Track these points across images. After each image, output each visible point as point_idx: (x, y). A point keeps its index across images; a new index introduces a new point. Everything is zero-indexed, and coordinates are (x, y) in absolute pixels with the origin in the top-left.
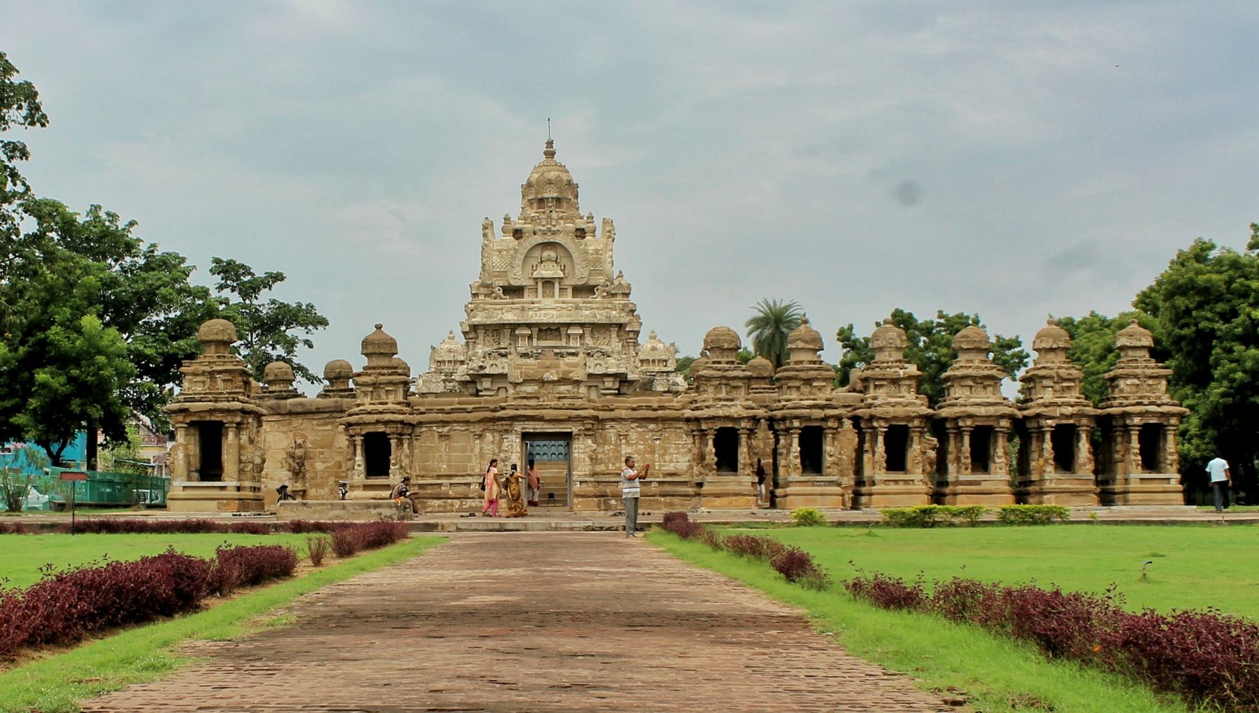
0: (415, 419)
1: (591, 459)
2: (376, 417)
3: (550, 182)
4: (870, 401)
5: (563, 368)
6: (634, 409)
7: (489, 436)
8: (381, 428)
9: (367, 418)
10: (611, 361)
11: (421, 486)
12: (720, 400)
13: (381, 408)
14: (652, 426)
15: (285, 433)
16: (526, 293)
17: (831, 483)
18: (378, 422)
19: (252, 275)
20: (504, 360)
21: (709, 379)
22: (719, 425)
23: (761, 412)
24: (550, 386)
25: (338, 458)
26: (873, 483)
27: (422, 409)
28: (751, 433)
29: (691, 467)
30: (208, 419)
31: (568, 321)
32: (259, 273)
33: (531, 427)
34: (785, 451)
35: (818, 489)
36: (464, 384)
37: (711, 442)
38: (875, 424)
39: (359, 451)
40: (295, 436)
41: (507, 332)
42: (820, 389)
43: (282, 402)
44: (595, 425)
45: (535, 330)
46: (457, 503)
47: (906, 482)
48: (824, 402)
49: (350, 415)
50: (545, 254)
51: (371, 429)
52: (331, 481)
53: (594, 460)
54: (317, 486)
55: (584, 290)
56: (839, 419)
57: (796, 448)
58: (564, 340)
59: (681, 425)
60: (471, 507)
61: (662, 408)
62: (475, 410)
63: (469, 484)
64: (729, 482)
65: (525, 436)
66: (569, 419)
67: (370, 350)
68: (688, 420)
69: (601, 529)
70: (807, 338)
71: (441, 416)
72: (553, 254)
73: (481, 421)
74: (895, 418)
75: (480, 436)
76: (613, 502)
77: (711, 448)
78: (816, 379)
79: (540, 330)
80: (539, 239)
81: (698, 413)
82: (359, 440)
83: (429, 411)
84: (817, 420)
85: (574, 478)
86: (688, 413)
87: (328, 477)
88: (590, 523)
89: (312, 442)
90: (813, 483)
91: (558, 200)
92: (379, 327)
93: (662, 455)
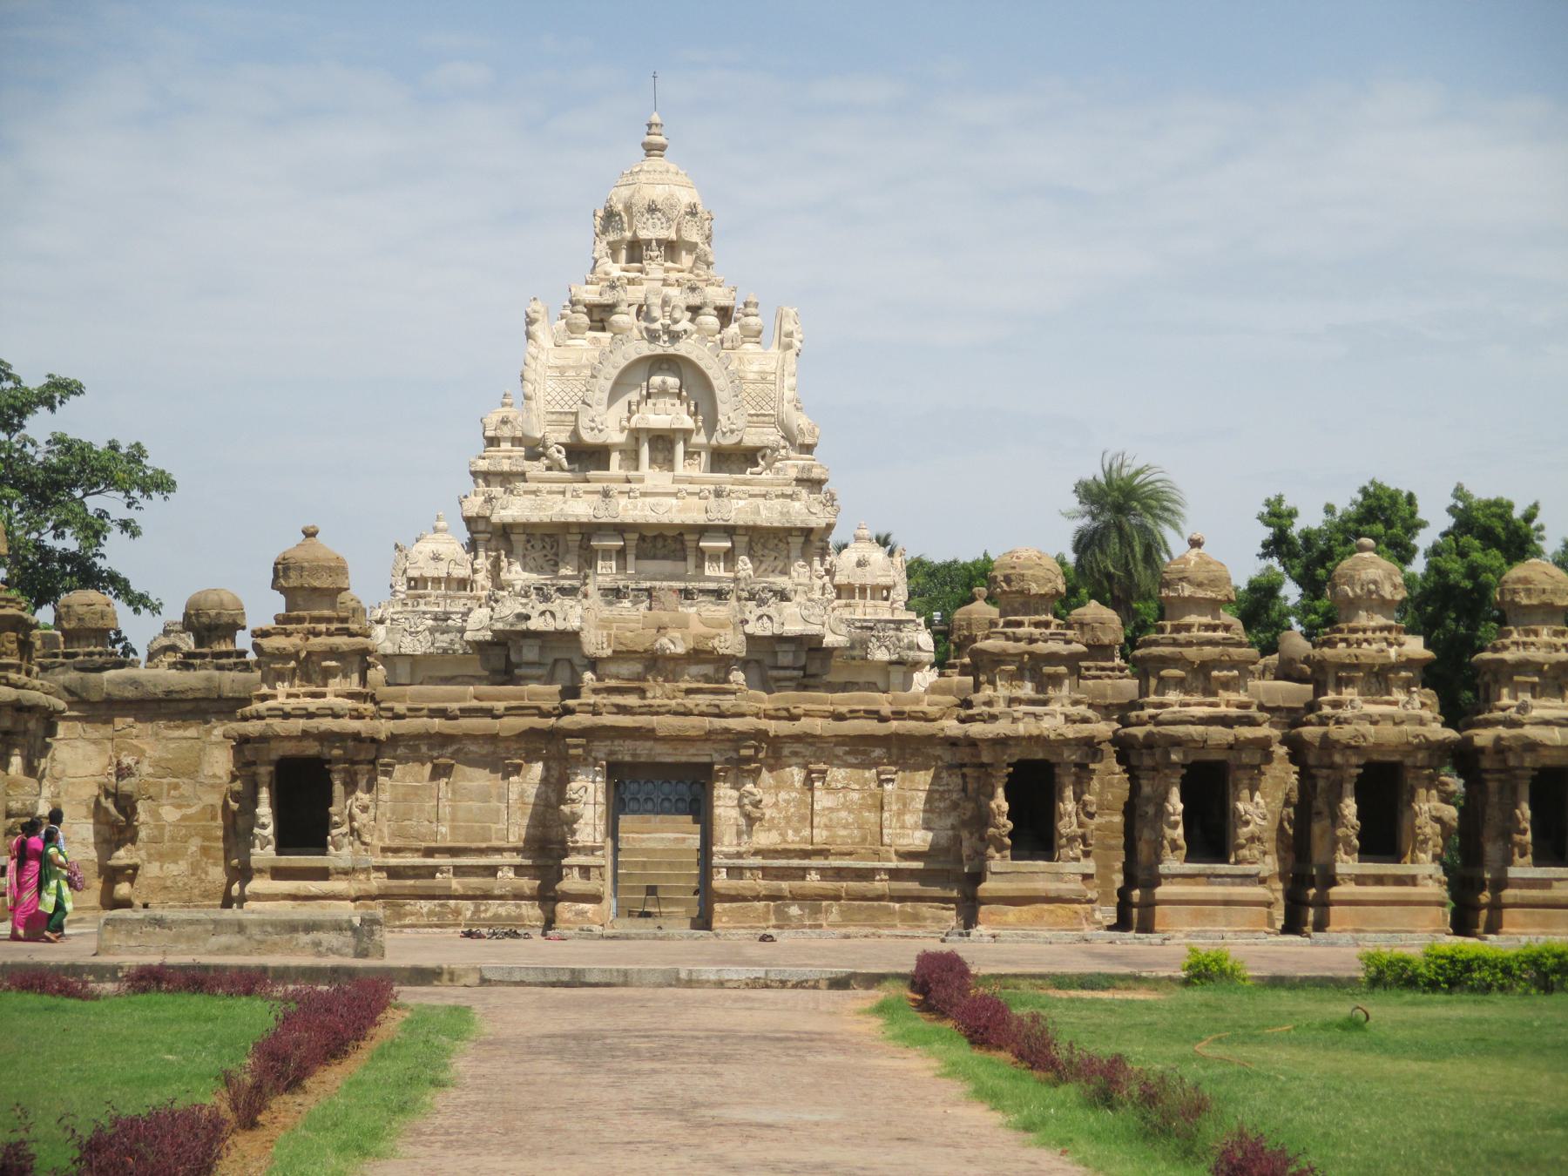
0: (384, 728)
2: (302, 724)
4: (1327, 710)
5: (697, 628)
6: (840, 717)
8: (312, 748)
9: (279, 725)
10: (790, 608)
11: (394, 873)
12: (1019, 701)
13: (312, 704)
14: (878, 752)
15: (95, 742)
16: (615, 458)
17: (1246, 878)
18: (306, 734)
19: (18, 381)
20: (568, 601)
21: (998, 659)
22: (1016, 754)
23: (1103, 729)
26: (1333, 881)
27: (400, 708)
28: (1083, 774)
29: (957, 840)
31: (701, 519)
32: (34, 381)
33: (626, 751)
34: (1151, 810)
35: (1218, 891)
36: (479, 646)
37: (1000, 792)
38: (1338, 759)
39: (264, 795)
40: (118, 750)
41: (574, 539)
42: (1227, 685)
43: (93, 676)
44: (755, 753)
45: (633, 537)
46: (468, 907)
47: (1400, 880)
48: (1234, 711)
49: (245, 719)
50: (656, 380)
51: (289, 749)
52: (194, 846)
54: (161, 857)
55: (734, 458)
56: (1263, 745)
57: (1175, 804)
58: (691, 562)
59: (938, 751)
60: (497, 917)
61: (899, 715)
62: (510, 711)
63: (492, 871)
64: (1037, 875)
66: (709, 736)
67: (294, 581)
68: (953, 742)
69: (783, 984)
70: (1201, 577)
71: (437, 724)
72: (672, 382)
74: (1378, 746)
76: (794, 910)
77: (1000, 802)
78: (1218, 664)
79: (642, 538)
80: (647, 349)
81: (976, 729)
82: (264, 771)
83: (414, 712)
84: (1218, 747)
85: (716, 860)
86: (951, 727)
87: (185, 839)
88: (759, 972)
89: (156, 764)
90: (1210, 878)
91: (671, 248)
92: (310, 534)
93: (900, 813)
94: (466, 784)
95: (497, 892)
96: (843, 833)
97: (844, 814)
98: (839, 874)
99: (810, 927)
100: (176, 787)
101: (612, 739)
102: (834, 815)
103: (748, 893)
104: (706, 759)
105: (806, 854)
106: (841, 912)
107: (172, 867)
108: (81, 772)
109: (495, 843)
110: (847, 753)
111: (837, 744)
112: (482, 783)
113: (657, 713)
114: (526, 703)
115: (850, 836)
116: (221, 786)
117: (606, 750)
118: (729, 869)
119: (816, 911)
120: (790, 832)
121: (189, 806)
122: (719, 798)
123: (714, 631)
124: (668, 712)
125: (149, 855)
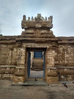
1: (55, 59)
6: (70, 40)
7: (15, 50)
24: (38, 30)
33: (30, 45)
53: (56, 60)
63: (6, 68)
65: (28, 50)
73: (12, 44)
75: (12, 49)
76: (62, 77)
94: (2, 52)
95: (6, 73)
96: (70, 61)
97: (70, 58)
98: (70, 69)
99: (66, 80)
101: (27, 42)
102: (68, 58)
103: (55, 75)
104: (46, 47)
105: (64, 65)
106: (72, 77)
109: (7, 63)
110: (71, 47)
111: (69, 45)
112: (5, 52)
113: (35, 38)
114: (13, 38)
115: (72, 62)
117: (26, 45)
118: (50, 69)
119: (66, 77)
120: (60, 61)
122: (48, 55)
123: (47, 24)
124: (38, 37)
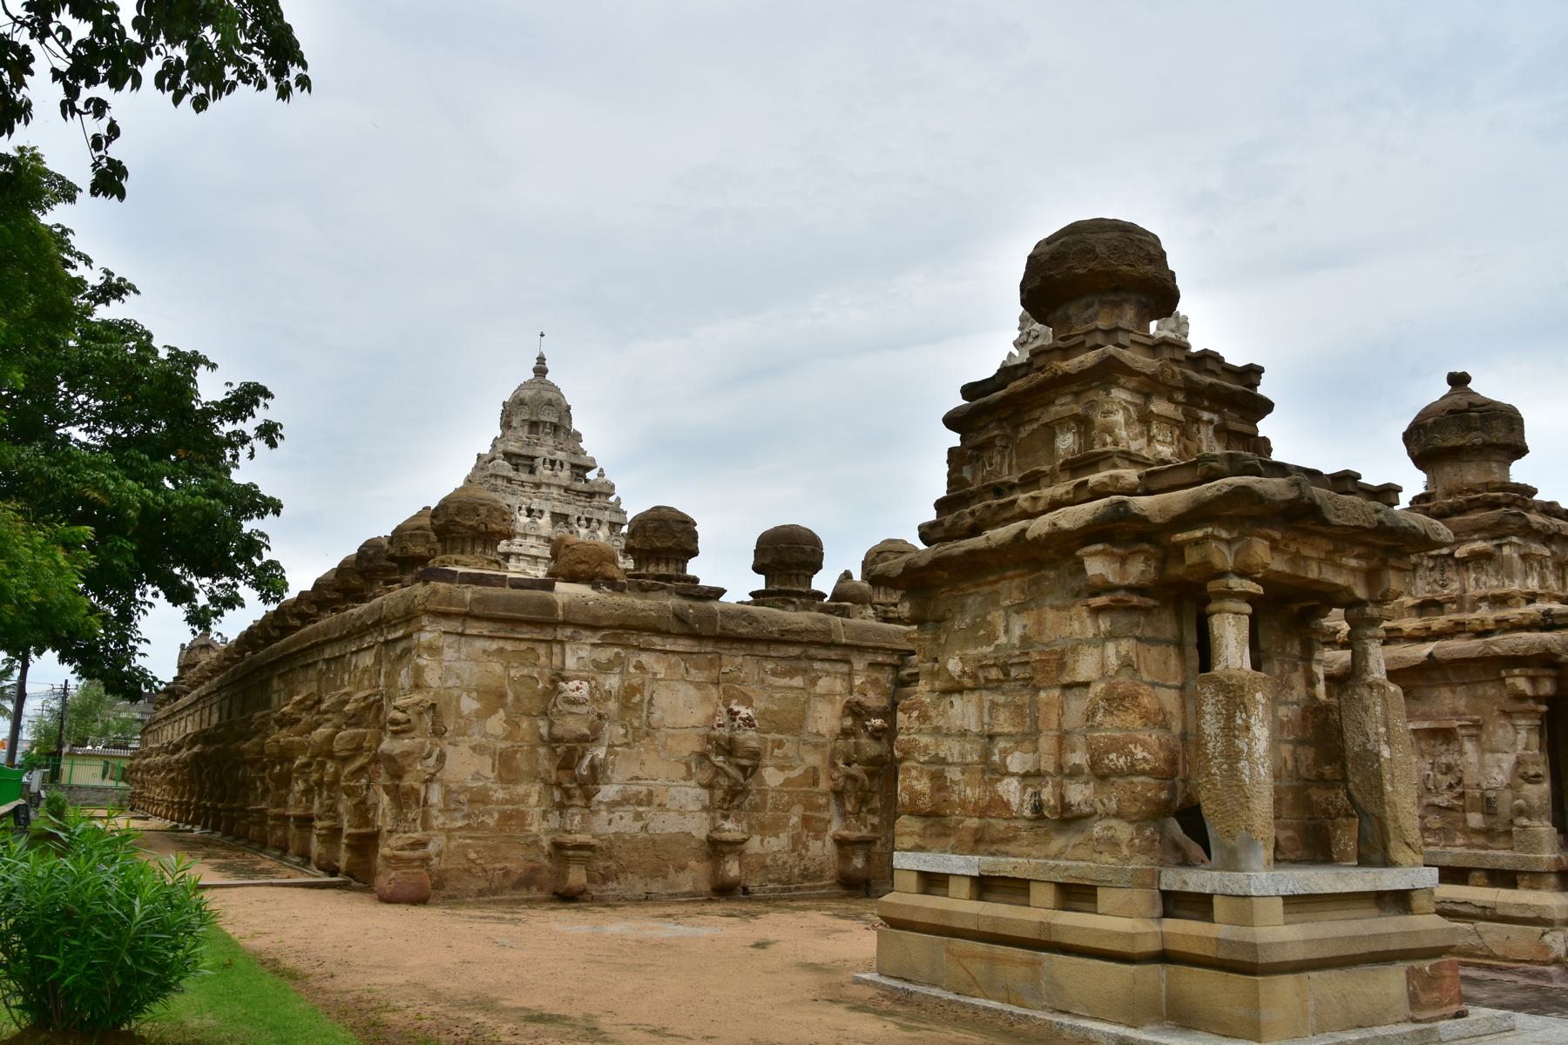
3: (550, 403)
25: (813, 759)
30: (1313, 573)
87: (790, 805)
91: (556, 428)
92: (1458, 381)
100: (780, 744)
107: (773, 840)
108: (681, 721)
116: (824, 745)
121: (791, 768)
125: (751, 827)
